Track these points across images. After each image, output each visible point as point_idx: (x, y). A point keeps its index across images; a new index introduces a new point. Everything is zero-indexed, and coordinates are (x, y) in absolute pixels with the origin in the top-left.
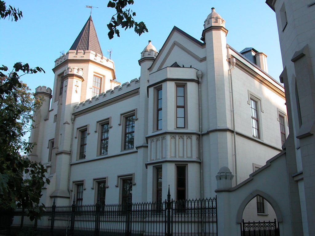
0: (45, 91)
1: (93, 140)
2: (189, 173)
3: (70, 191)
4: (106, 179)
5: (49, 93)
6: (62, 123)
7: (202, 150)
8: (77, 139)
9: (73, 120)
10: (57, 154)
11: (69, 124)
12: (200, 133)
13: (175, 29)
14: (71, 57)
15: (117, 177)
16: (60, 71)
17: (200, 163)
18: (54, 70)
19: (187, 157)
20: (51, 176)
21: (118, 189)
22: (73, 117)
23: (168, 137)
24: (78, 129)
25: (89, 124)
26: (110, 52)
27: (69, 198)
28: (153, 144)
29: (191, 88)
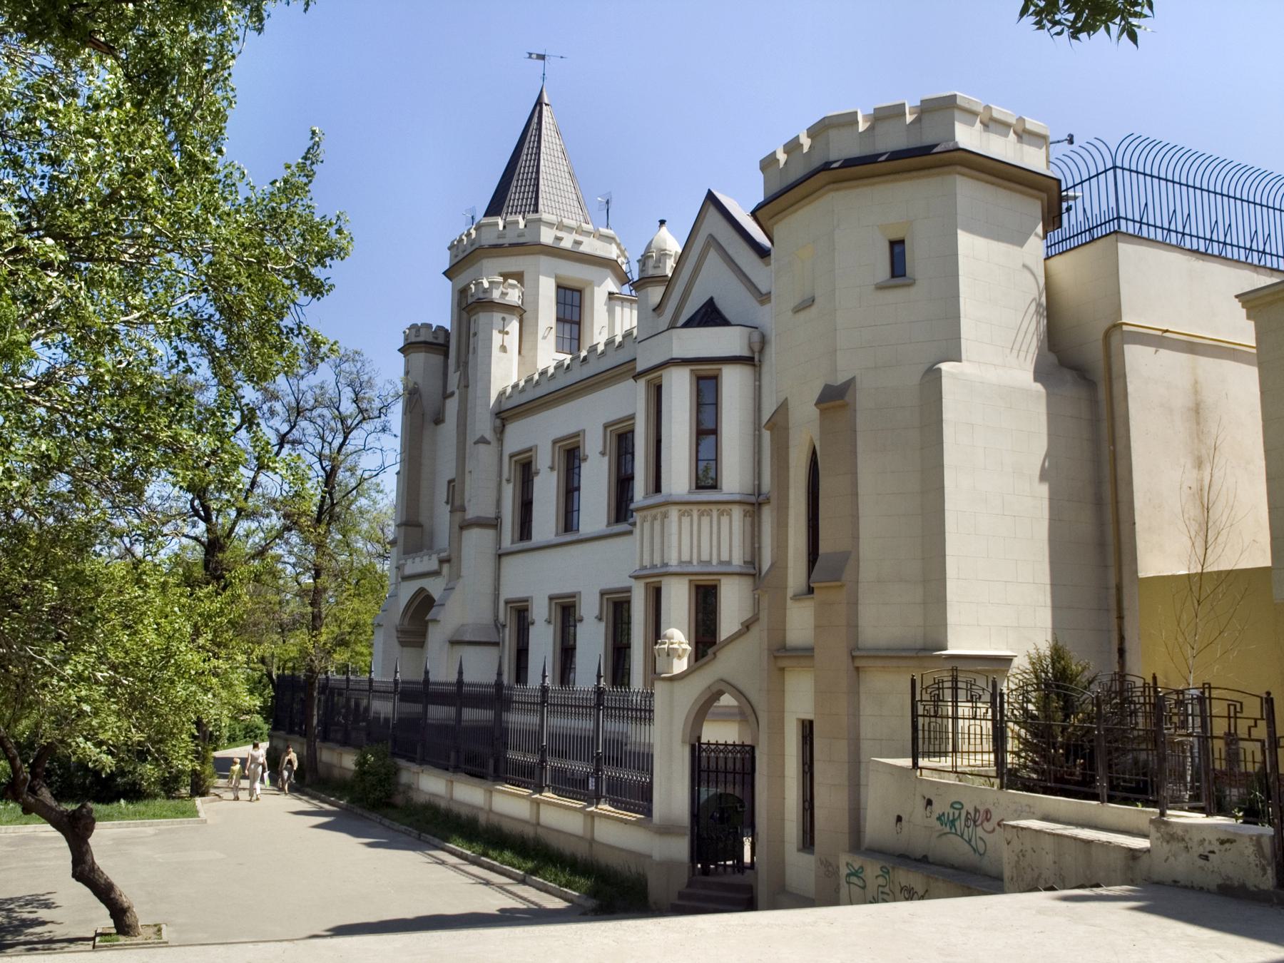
0: (430, 339)
1: (547, 488)
2: (722, 600)
3: (499, 626)
4: (576, 600)
5: (441, 340)
6: (470, 442)
7: (760, 543)
8: (511, 485)
9: (500, 432)
10: (462, 528)
11: (488, 443)
12: (753, 499)
13: (711, 198)
14: (489, 238)
15: (597, 596)
16: (463, 279)
17: (754, 575)
18: (448, 274)
19: (721, 563)
20: (450, 586)
21: (603, 625)
22: (498, 422)
23: (674, 513)
24: (511, 456)
25: (536, 446)
26: (607, 202)
27: (496, 644)
28: (647, 526)
29: (734, 382)
